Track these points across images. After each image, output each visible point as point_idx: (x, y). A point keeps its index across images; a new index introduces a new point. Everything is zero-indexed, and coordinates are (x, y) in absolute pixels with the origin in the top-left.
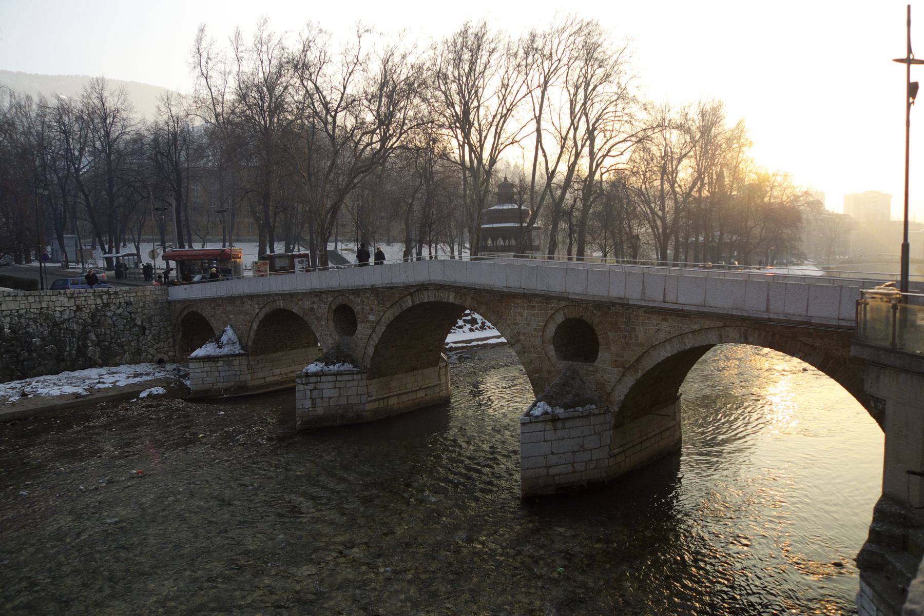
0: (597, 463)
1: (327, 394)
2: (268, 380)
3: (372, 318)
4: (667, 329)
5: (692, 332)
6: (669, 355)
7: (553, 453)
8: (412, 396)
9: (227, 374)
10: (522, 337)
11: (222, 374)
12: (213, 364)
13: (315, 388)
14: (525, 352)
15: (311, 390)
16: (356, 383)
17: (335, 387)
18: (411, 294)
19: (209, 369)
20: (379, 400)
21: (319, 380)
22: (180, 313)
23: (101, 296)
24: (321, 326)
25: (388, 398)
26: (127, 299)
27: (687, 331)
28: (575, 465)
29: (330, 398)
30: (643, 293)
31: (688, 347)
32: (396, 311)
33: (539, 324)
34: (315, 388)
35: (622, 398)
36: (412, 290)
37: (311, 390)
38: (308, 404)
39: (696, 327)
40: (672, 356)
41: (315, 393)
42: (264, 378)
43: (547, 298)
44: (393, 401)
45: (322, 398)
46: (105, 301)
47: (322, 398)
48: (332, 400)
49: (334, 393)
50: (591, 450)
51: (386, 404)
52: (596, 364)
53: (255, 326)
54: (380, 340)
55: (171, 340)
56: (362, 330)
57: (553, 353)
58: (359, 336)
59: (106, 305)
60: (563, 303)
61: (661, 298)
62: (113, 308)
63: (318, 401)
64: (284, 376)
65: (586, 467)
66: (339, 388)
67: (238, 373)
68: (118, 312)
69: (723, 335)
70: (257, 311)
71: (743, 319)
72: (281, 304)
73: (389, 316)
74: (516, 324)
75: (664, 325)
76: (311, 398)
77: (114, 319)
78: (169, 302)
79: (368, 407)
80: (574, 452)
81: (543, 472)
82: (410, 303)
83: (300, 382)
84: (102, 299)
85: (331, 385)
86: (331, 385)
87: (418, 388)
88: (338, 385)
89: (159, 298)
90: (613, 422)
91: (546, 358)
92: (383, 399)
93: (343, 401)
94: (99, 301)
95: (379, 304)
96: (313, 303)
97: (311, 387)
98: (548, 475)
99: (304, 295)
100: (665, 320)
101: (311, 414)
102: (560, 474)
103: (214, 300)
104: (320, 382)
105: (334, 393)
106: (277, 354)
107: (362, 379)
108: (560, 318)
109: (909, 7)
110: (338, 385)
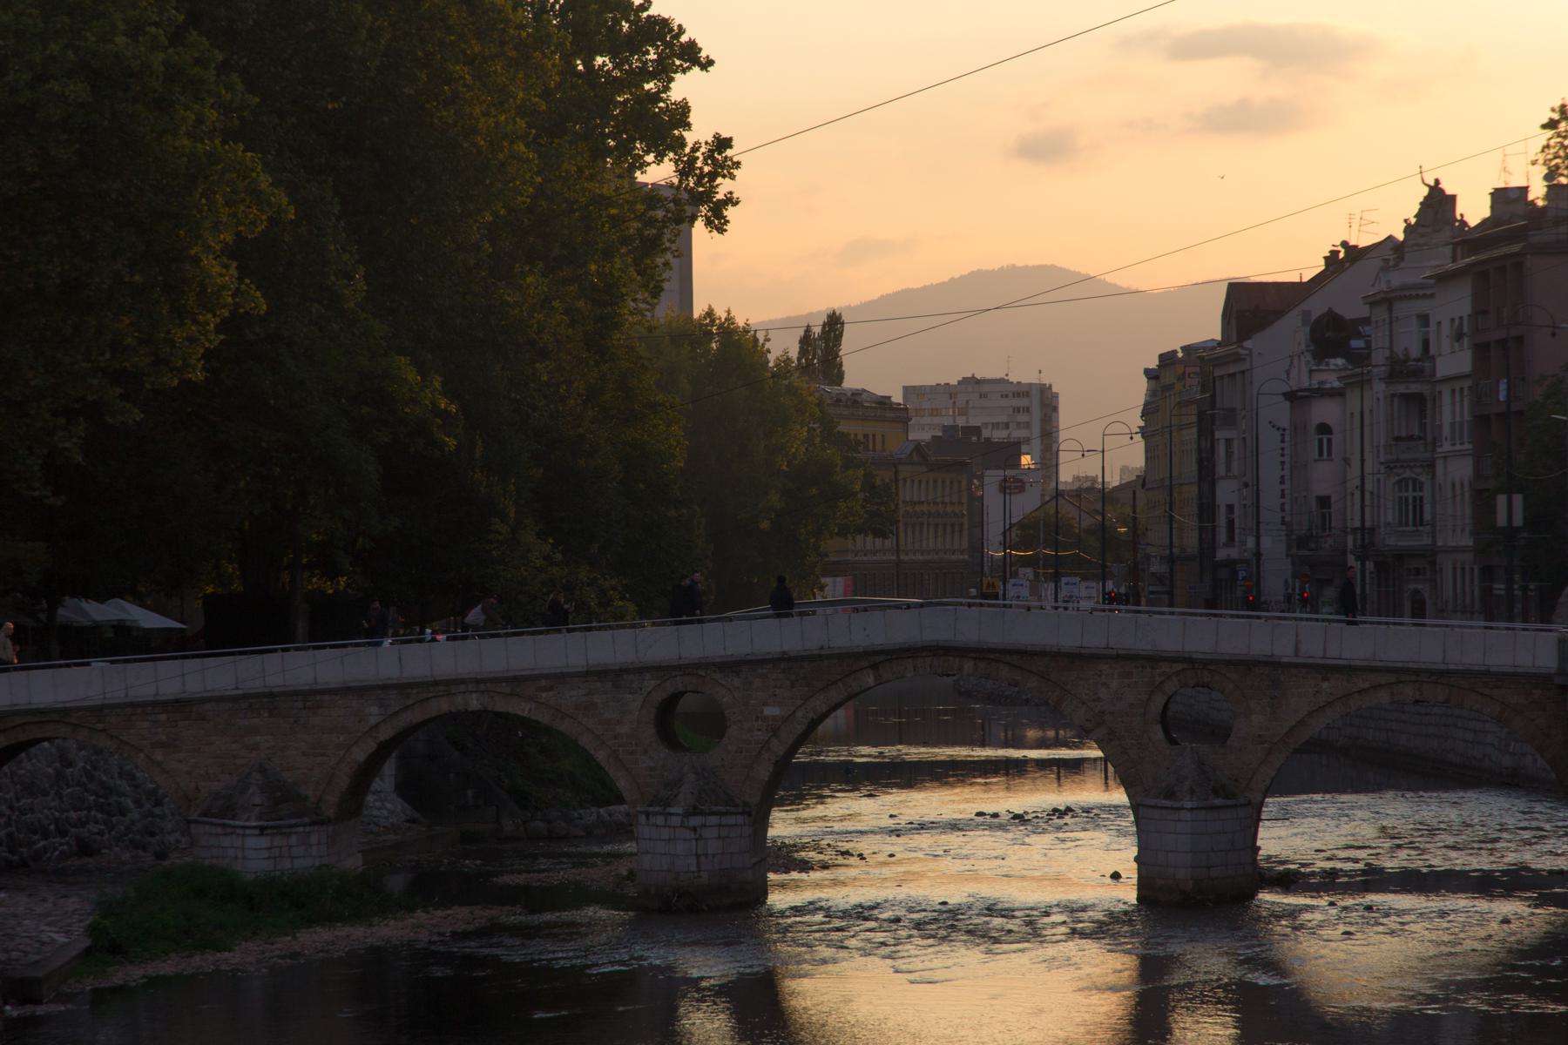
3: (770, 711)
5: (1358, 692)
17: (719, 837)
18: (874, 667)
29: (714, 856)
30: (1297, 649)
39: (1366, 685)
47: (706, 855)
60: (1179, 667)
63: (703, 858)
70: (373, 721)
71: (1417, 672)
74: (1099, 699)
75: (1325, 685)
76: (696, 855)
95: (793, 685)
99: (559, 679)
100: (1325, 679)
107: (745, 825)
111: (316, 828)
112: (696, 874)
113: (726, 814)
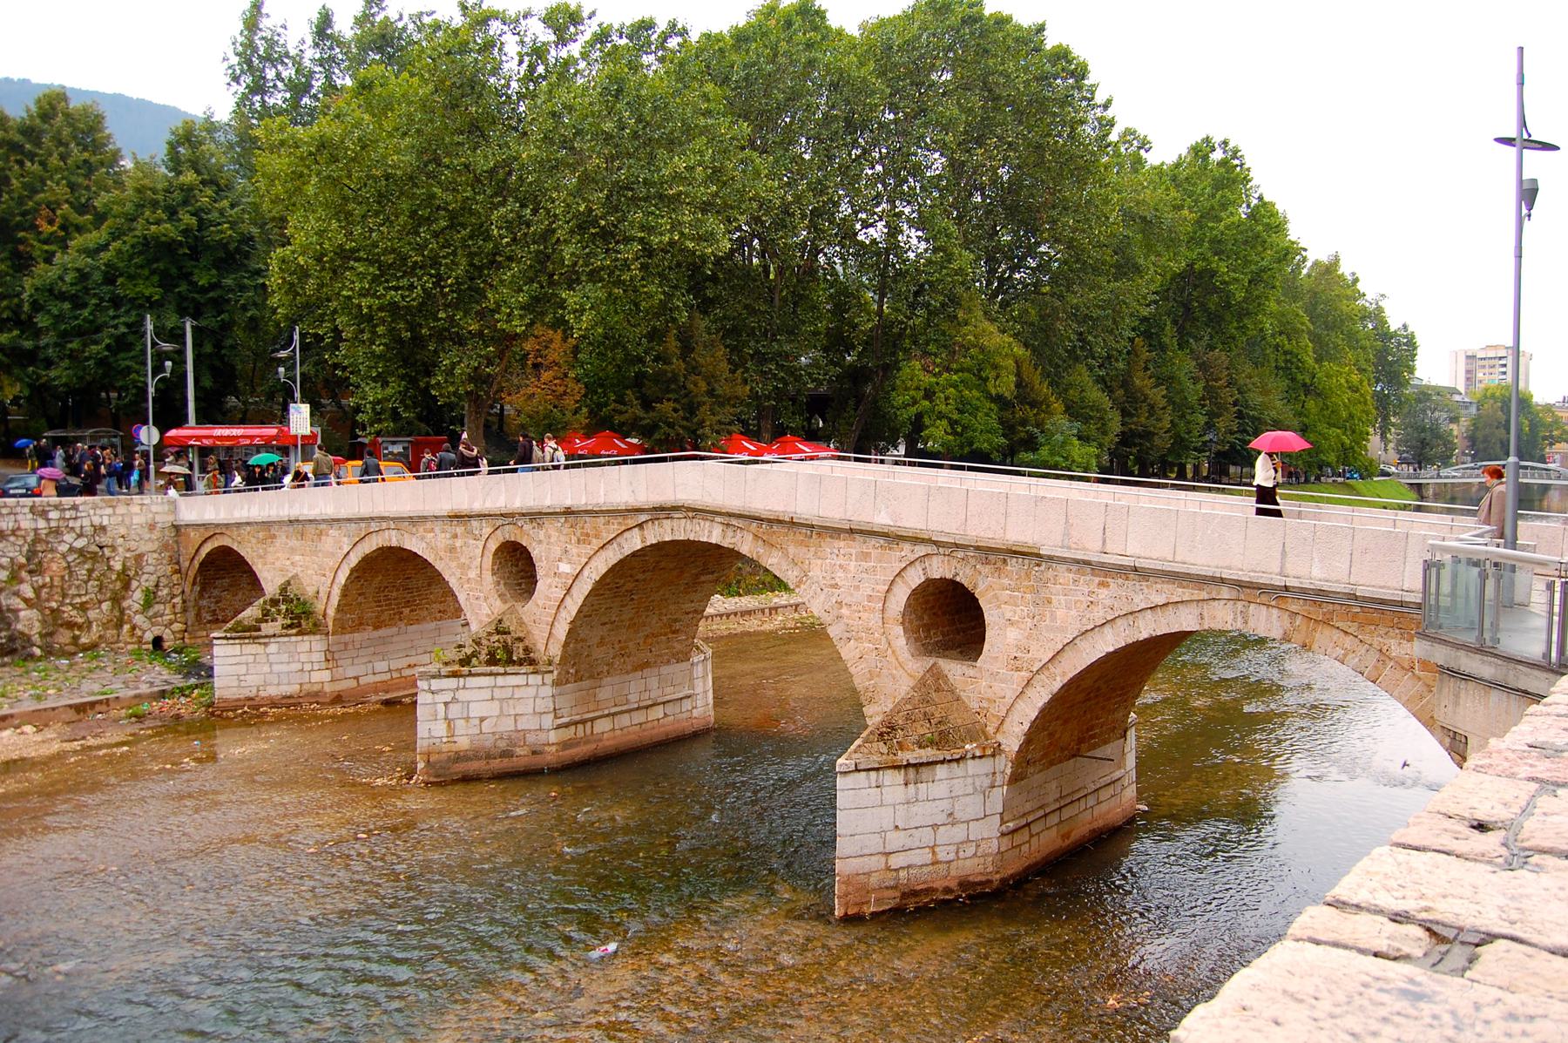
0: (978, 846)
1: (476, 710)
2: (363, 681)
4: (1108, 602)
6: (1111, 649)
7: (897, 827)
8: (639, 717)
9: (284, 668)
10: (845, 611)
11: (276, 668)
12: (260, 649)
13: (455, 700)
14: (849, 639)
15: (446, 704)
16: (531, 691)
19: (251, 659)
20: (576, 723)
21: (461, 684)
22: (197, 551)
23: (44, 514)
24: (468, 580)
25: (592, 720)
26: (96, 521)
27: (1143, 606)
28: (937, 849)
29: (482, 720)
30: (1067, 534)
31: (1144, 635)
32: (612, 557)
33: (878, 587)
34: (455, 700)
35: (1026, 726)
36: (643, 517)
37: (446, 704)
38: (440, 729)
39: (1160, 600)
40: (1116, 652)
41: (455, 711)
42: (357, 678)
43: (892, 538)
44: (602, 726)
45: (468, 719)
46: (53, 524)
47: (468, 719)
48: (485, 724)
49: (492, 709)
50: (968, 822)
51: (588, 731)
52: (979, 663)
53: (342, 577)
54: (580, 611)
55: (178, 600)
56: (547, 587)
57: (902, 641)
58: (540, 603)
59: (56, 532)
60: (921, 550)
61: (1098, 545)
62: (69, 538)
63: (460, 724)
64: (395, 675)
65: (957, 853)
66: (501, 700)
67: (308, 667)
68: (80, 543)
69: (1205, 614)
72: (393, 539)
73: (601, 566)
74: (836, 586)
75: (1103, 593)
77: (70, 559)
78: (177, 528)
79: (553, 737)
80: (935, 827)
81: (876, 863)
82: (639, 542)
83: (426, 688)
84: (48, 520)
85: (486, 694)
86: (486, 694)
87: (650, 702)
88: (498, 693)
89: (158, 518)
90: (1009, 771)
91: (890, 651)
92: (583, 722)
93: (507, 725)
94: (42, 524)
96: (455, 536)
97: (447, 697)
98: (888, 869)
100: (1102, 584)
101: (445, 748)
102: (909, 867)
103: (267, 525)
104: (464, 688)
105: (492, 709)
106: (382, 632)
107: (544, 684)
108: (915, 578)
109: (1521, 49)
110: (498, 693)
111: (306, 638)
112: (445, 740)
113: (505, 674)
